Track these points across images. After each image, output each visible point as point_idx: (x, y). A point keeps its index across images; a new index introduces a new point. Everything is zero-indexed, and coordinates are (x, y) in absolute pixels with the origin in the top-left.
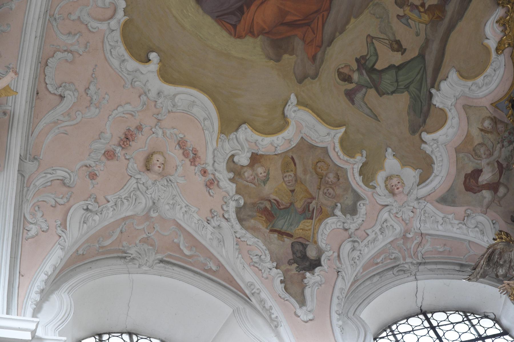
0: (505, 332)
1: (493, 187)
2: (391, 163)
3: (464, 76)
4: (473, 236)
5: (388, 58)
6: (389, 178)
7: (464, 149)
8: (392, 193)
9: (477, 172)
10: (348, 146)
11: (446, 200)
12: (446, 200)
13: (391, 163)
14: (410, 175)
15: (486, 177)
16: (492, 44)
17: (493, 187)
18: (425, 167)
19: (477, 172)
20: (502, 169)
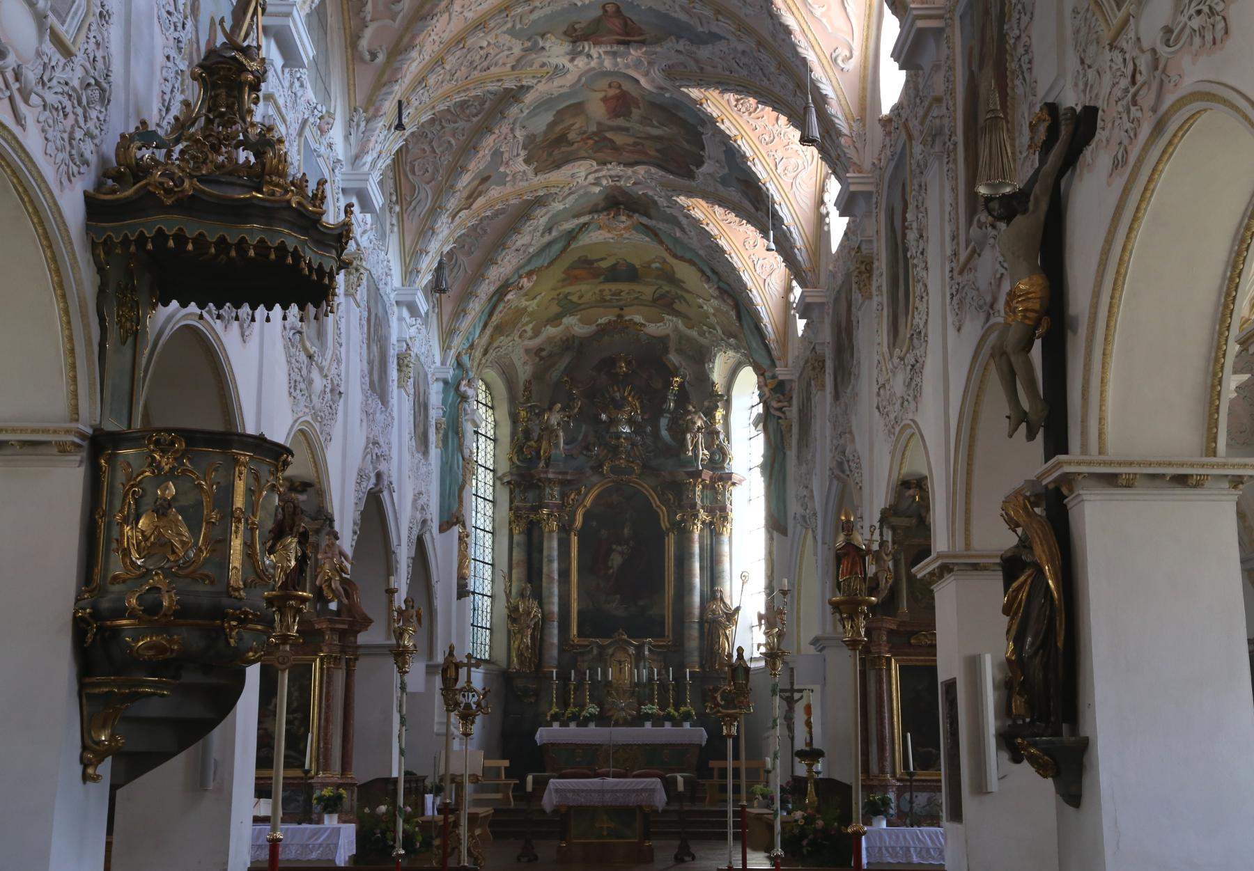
0: (492, 408)
1: (542, 358)
2: (531, 326)
3: (579, 320)
4: (520, 371)
5: (575, 298)
6: (525, 331)
7: (550, 340)
8: (520, 337)
9: (542, 350)
10: (531, 314)
11: (527, 351)
12: (527, 351)
13: (531, 326)
14: (530, 333)
15: (544, 354)
16: (600, 321)
17: (542, 358)
18: (536, 333)
19: (542, 350)
20: (550, 356)
